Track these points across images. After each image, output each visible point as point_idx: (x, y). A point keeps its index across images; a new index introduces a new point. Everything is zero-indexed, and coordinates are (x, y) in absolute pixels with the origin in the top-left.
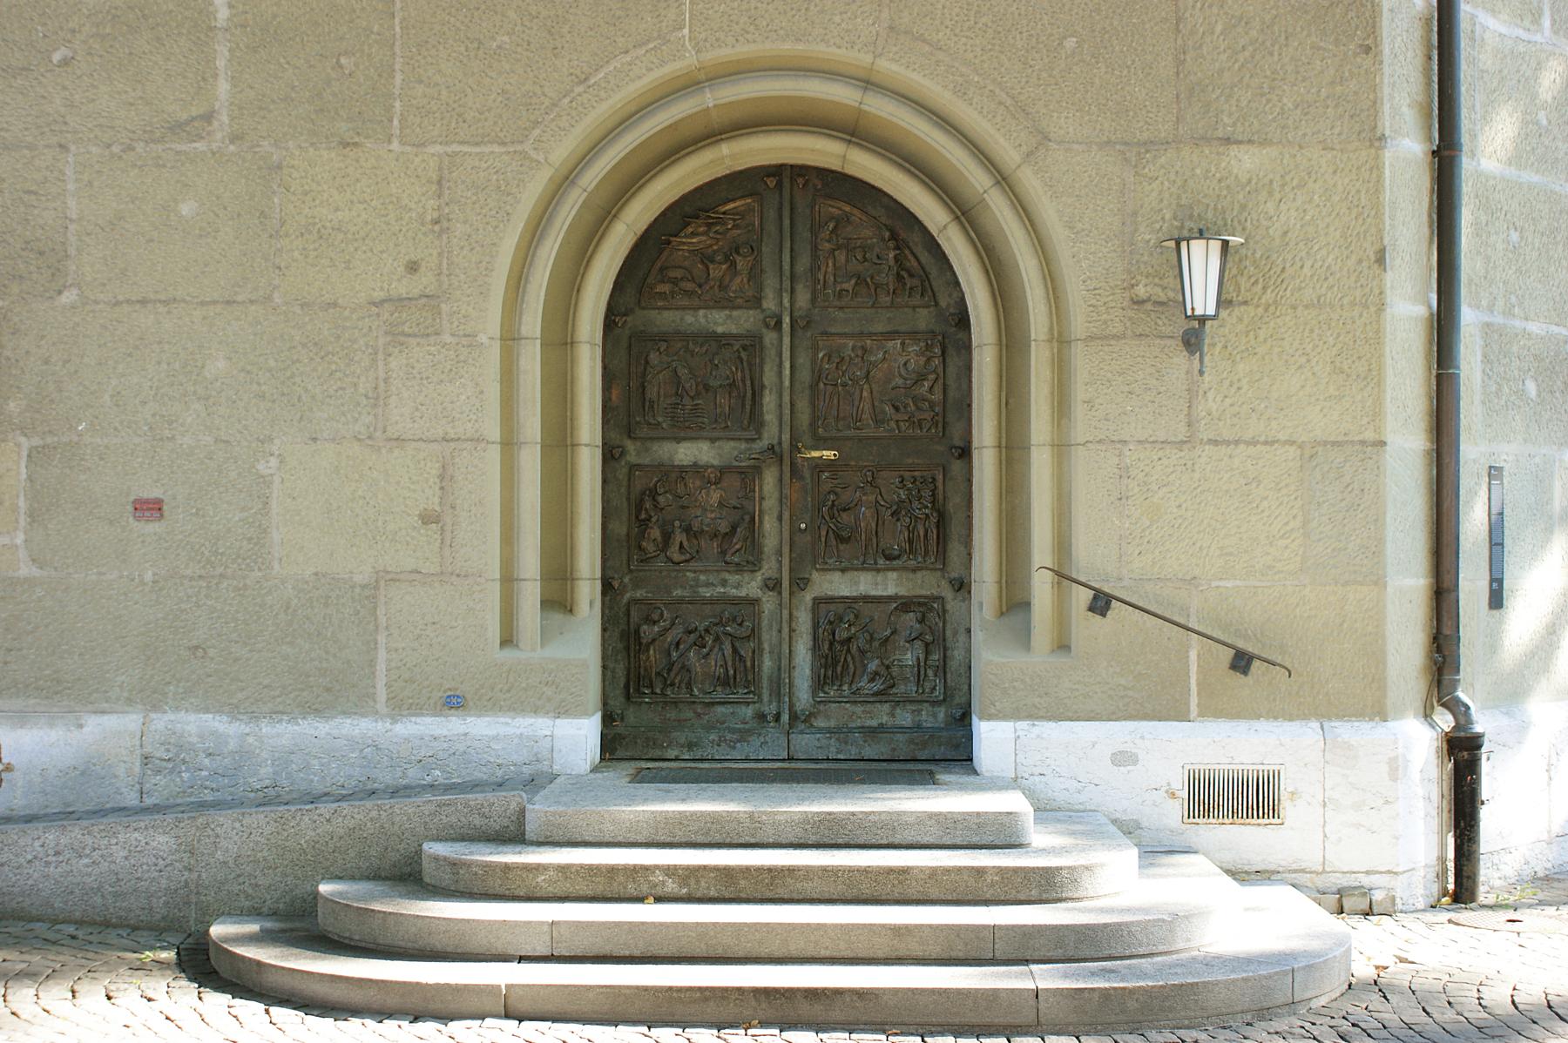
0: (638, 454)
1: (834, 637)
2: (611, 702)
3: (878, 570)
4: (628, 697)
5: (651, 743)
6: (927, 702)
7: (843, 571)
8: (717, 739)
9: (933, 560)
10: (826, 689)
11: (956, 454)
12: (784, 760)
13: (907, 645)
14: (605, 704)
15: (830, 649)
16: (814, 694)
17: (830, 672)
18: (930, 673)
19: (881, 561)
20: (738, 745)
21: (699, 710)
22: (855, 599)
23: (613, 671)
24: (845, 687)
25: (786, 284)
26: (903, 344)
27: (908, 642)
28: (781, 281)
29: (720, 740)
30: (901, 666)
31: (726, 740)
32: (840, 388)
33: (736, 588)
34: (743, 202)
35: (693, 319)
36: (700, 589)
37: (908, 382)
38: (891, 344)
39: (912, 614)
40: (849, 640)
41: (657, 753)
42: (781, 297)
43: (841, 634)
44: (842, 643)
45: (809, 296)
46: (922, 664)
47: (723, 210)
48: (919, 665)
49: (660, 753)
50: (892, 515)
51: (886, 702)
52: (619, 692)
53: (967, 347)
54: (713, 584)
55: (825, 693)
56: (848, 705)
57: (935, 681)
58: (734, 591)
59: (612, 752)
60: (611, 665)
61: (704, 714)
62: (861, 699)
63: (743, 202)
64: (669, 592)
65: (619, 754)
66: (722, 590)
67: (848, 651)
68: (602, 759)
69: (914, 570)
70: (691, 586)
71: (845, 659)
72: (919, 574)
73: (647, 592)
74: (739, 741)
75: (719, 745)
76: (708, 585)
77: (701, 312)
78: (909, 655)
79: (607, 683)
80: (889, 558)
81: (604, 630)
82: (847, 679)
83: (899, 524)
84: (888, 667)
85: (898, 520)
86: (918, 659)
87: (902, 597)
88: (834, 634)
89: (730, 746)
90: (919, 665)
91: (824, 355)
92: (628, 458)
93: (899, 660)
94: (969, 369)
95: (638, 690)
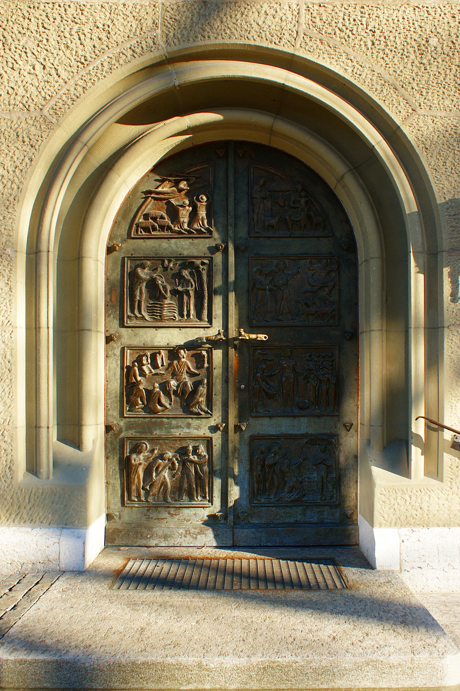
0: (130, 338)
1: (264, 463)
2: (112, 506)
3: (295, 417)
4: (123, 504)
5: (139, 535)
6: (328, 505)
7: (270, 417)
8: (184, 532)
9: (332, 409)
10: (259, 498)
11: (348, 337)
12: (230, 546)
13: (314, 467)
14: (108, 508)
15: (262, 470)
16: (251, 501)
17: (262, 486)
18: (330, 487)
19: (296, 411)
20: (199, 536)
21: (172, 512)
22: (278, 437)
23: (114, 486)
24: (272, 497)
25: (231, 221)
26: (311, 262)
27: (315, 465)
28: (227, 220)
29: (186, 533)
30: (310, 482)
31: (190, 533)
32: (268, 292)
33: (197, 429)
34: (201, 167)
35: (167, 245)
36: (172, 430)
37: (315, 288)
38: (303, 262)
39: (317, 446)
40: (275, 464)
41: (143, 542)
42: (227, 230)
43: (270, 461)
44: (270, 466)
45: (246, 229)
46: (325, 480)
47: (188, 172)
48: (323, 480)
49: (145, 542)
50: (304, 379)
51: (300, 506)
52: (118, 499)
53: (354, 265)
54: (180, 427)
55: (259, 501)
56: (274, 508)
57: (333, 491)
58: (195, 431)
59: (113, 541)
60: (112, 481)
61: (175, 515)
62: (283, 505)
63: (201, 167)
64: (151, 433)
65: (117, 542)
66: (187, 431)
67: (274, 471)
68: (106, 547)
69: (319, 416)
70: (166, 428)
71: (272, 478)
72: (322, 419)
73: (135, 432)
74: (199, 533)
75: (185, 537)
76: (178, 427)
77: (173, 241)
78: (315, 475)
79: (109, 494)
80: (301, 409)
81: (107, 458)
82: (274, 491)
83: (309, 385)
84: (301, 482)
85: (308, 382)
86: (322, 477)
87: (311, 435)
88: (264, 460)
89: (193, 538)
90: (323, 480)
91: (258, 269)
92: (123, 340)
93: (309, 478)
94: (356, 278)
95: (129, 498)
